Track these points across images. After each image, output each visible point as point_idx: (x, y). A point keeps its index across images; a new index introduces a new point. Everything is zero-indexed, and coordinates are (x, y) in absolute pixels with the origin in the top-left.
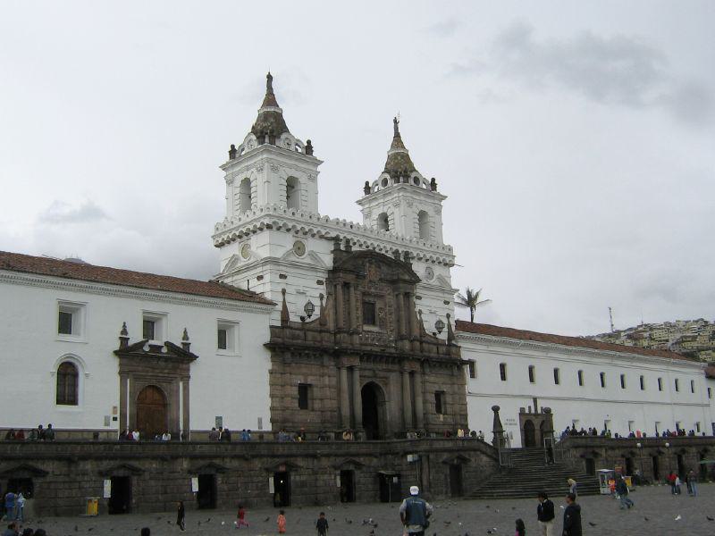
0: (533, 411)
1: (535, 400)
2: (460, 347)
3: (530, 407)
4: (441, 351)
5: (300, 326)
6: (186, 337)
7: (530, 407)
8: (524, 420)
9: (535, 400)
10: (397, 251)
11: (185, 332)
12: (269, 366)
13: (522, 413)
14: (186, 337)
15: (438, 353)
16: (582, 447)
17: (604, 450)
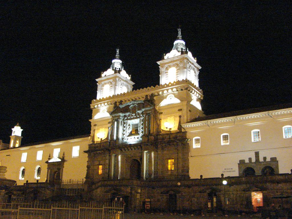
0: (254, 160)
1: (257, 154)
2: (186, 132)
3: (250, 159)
4: (171, 137)
5: (99, 142)
6: (64, 155)
7: (250, 159)
8: (243, 168)
9: (257, 154)
10: (147, 96)
11: (64, 153)
12: (87, 159)
13: (242, 162)
14: (64, 155)
15: (170, 138)
16: (109, 186)
17: (130, 188)
